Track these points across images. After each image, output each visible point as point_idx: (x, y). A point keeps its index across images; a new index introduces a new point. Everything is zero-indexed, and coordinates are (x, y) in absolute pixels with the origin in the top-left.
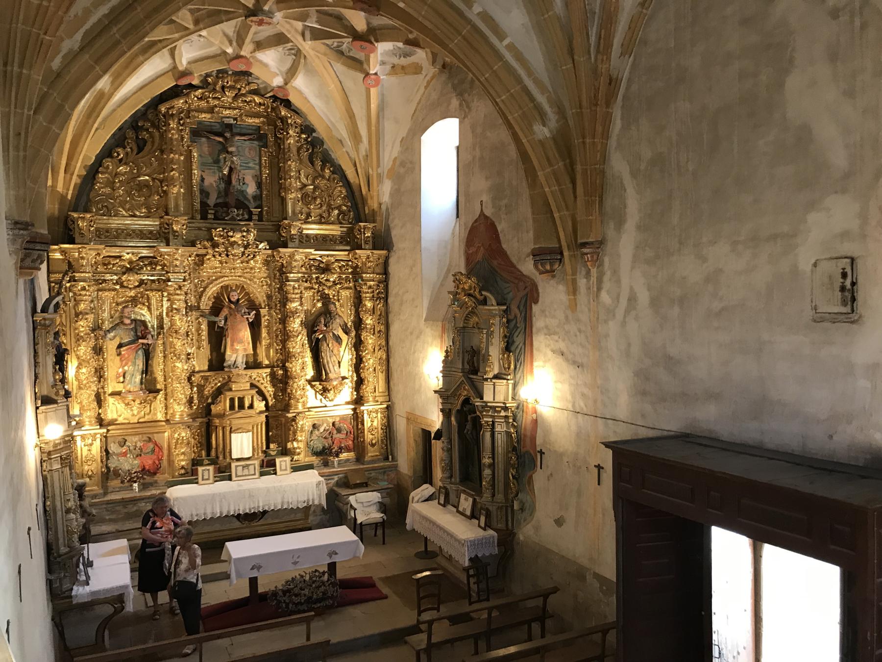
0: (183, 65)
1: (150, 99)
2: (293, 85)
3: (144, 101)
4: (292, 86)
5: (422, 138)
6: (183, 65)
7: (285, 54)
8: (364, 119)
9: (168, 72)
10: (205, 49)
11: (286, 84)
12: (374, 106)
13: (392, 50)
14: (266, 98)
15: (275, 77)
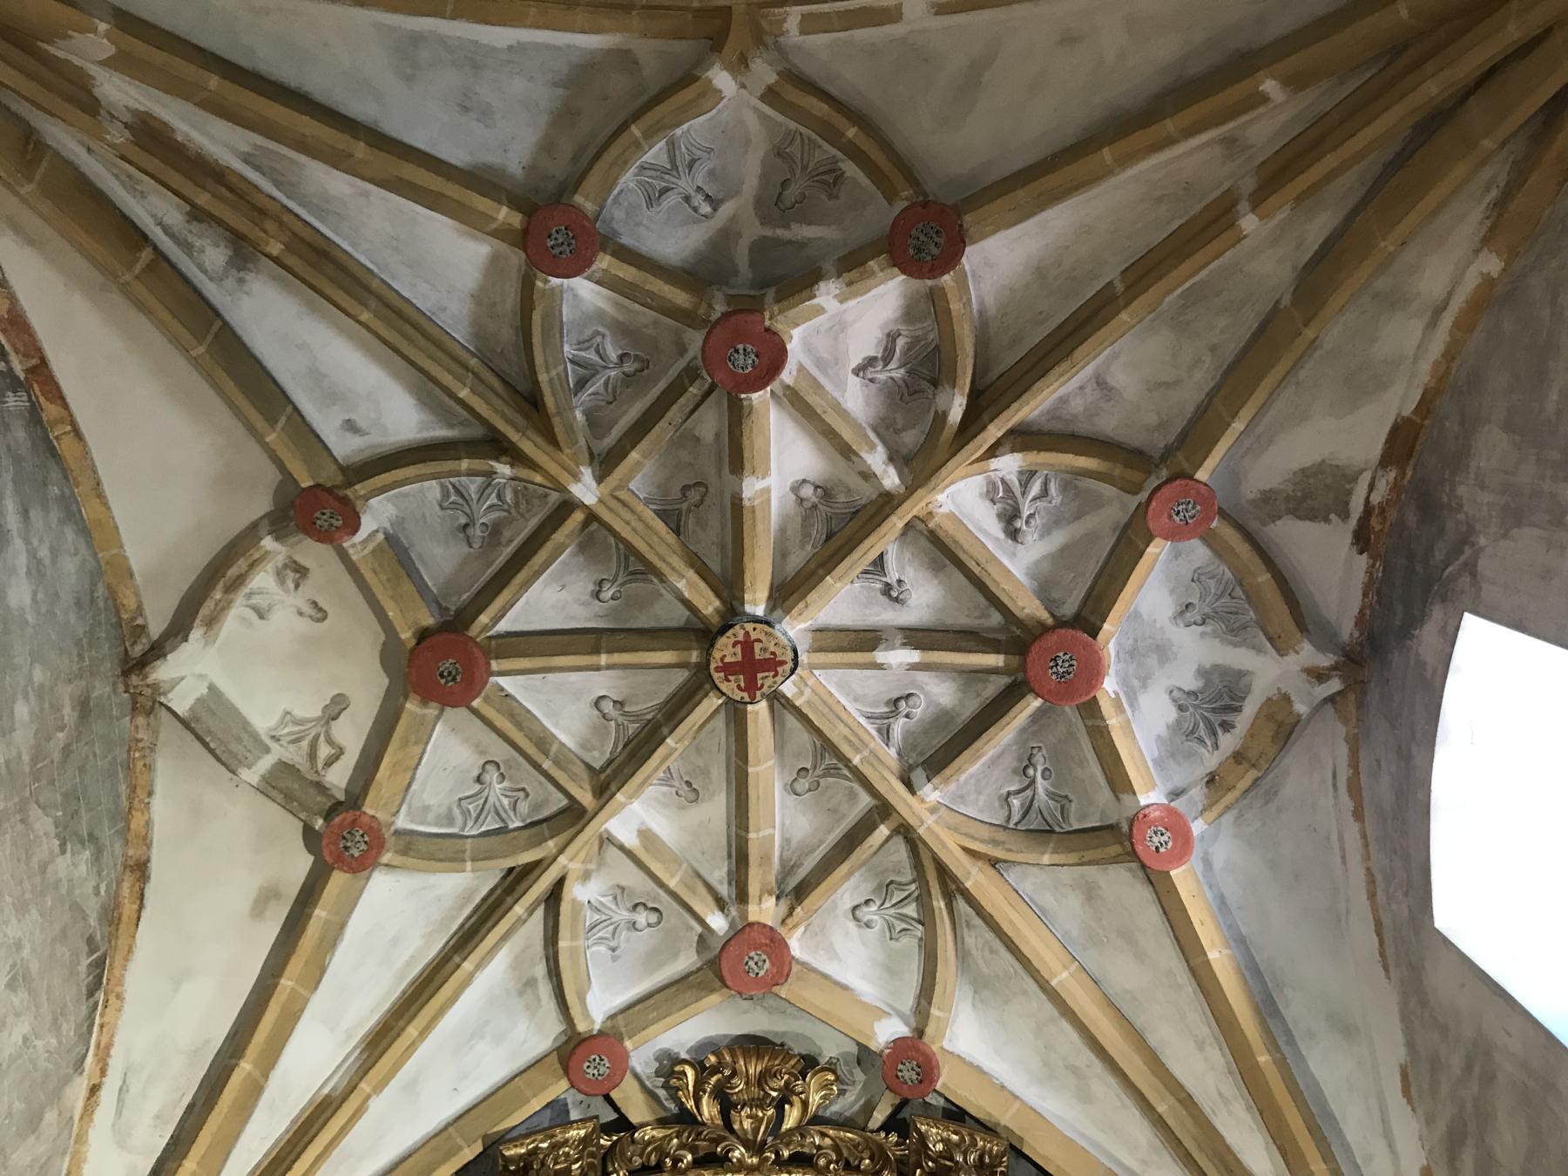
0: (593, 1022)
1: (478, 1148)
2: (946, 1044)
3: (460, 1149)
4: (942, 1048)
5: (1437, 925)
6: (586, 1014)
7: (890, 927)
8: (1231, 1088)
9: (551, 1053)
10: (661, 965)
11: (920, 1032)
12: (1218, 956)
13: (1178, 723)
14: (872, 1132)
15: (879, 1020)
